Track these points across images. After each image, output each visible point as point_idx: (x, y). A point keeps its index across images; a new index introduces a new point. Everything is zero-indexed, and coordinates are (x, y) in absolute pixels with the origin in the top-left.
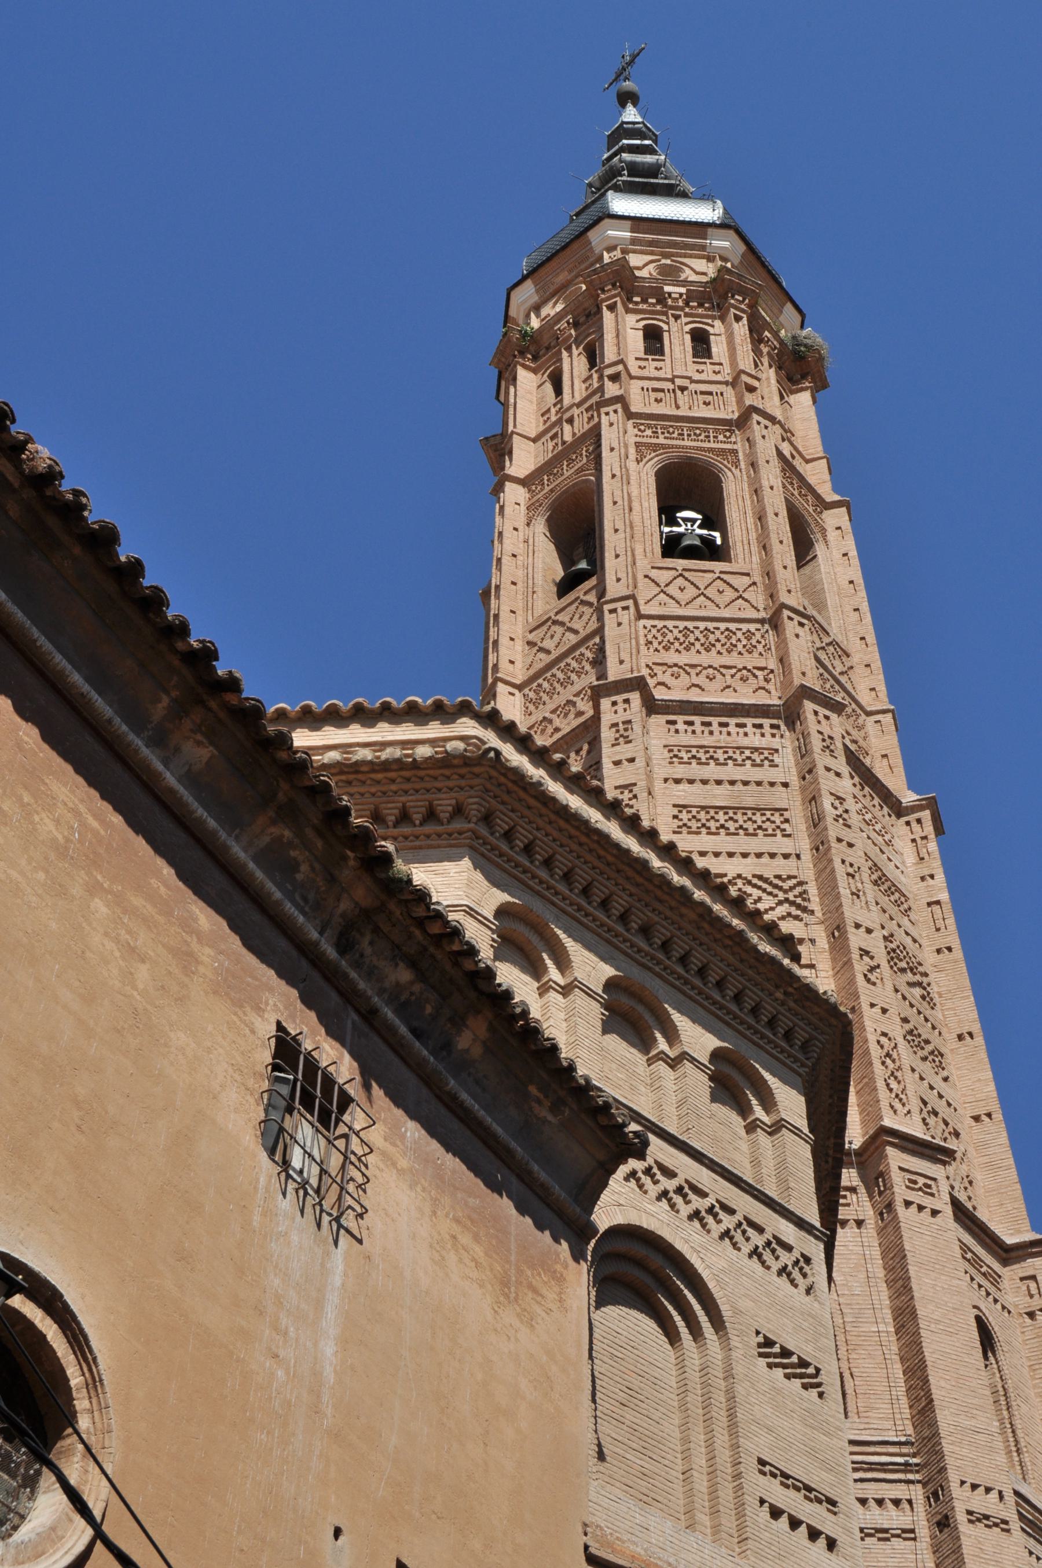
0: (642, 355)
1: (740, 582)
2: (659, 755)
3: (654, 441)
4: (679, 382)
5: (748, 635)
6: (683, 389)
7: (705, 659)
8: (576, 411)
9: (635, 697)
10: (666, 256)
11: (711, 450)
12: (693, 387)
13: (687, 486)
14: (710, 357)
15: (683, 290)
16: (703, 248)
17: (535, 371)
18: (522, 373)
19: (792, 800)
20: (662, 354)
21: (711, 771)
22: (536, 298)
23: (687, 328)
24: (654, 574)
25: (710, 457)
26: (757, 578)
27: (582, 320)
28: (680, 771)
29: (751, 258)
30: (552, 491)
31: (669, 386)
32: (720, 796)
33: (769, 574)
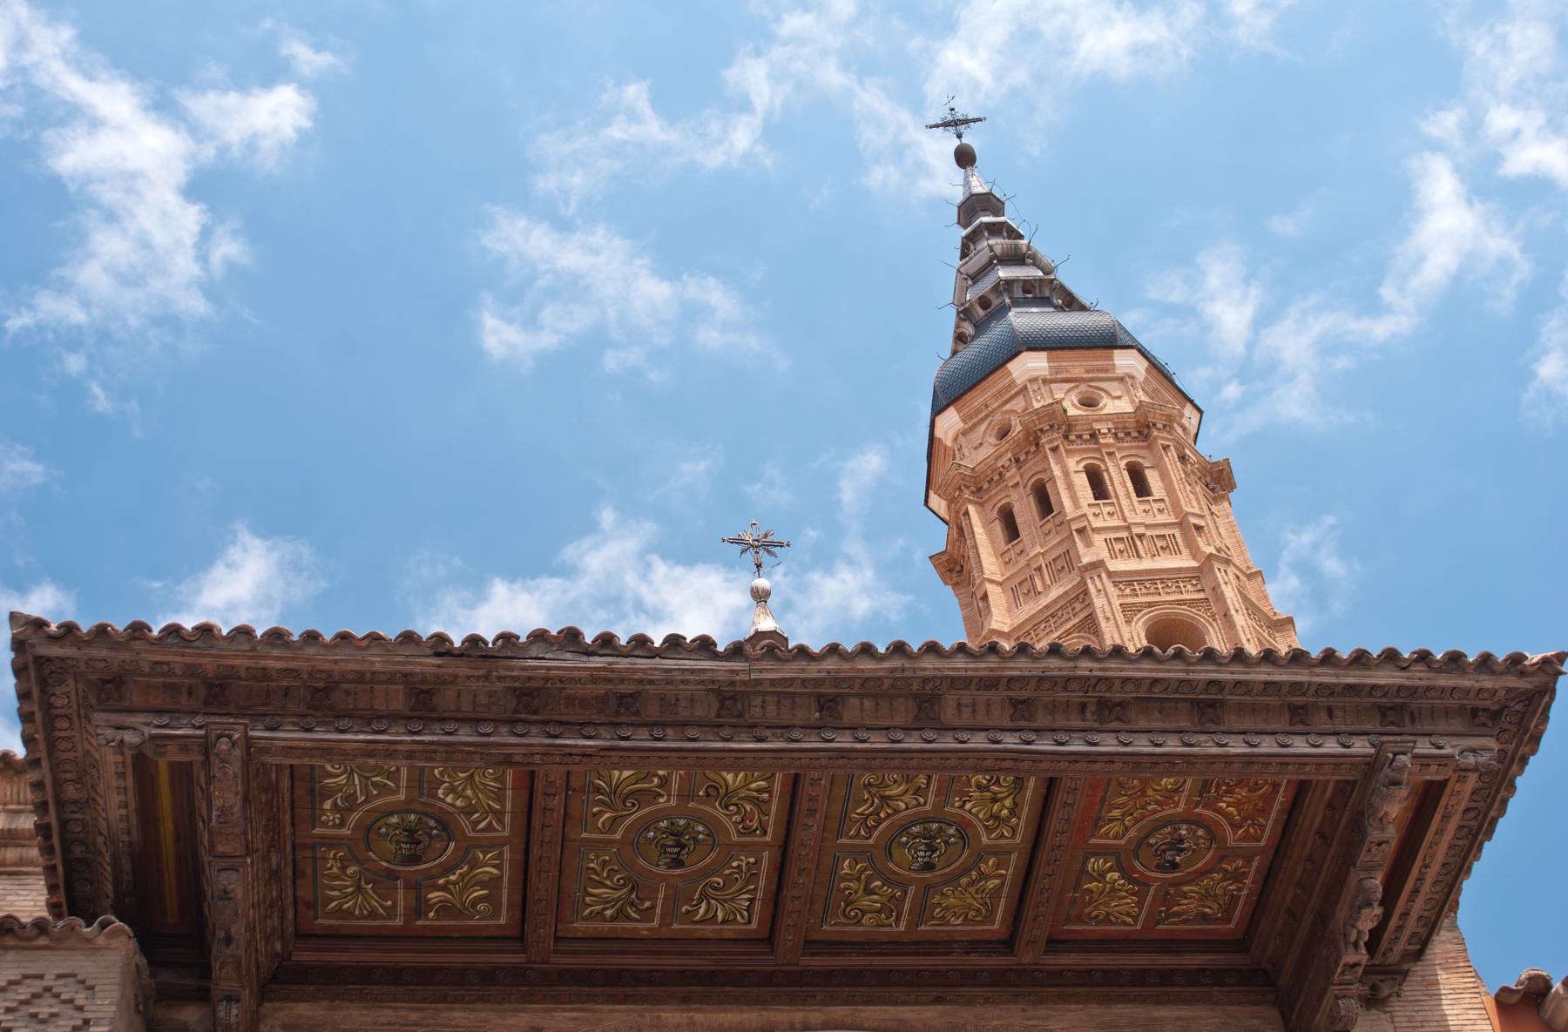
0: (1093, 501)
4: (1136, 530)
6: (1140, 536)
12: (1149, 533)
14: (1149, 494)
23: (1123, 464)
25: (1184, 610)
27: (1022, 458)
29: (1155, 372)
31: (1125, 534)
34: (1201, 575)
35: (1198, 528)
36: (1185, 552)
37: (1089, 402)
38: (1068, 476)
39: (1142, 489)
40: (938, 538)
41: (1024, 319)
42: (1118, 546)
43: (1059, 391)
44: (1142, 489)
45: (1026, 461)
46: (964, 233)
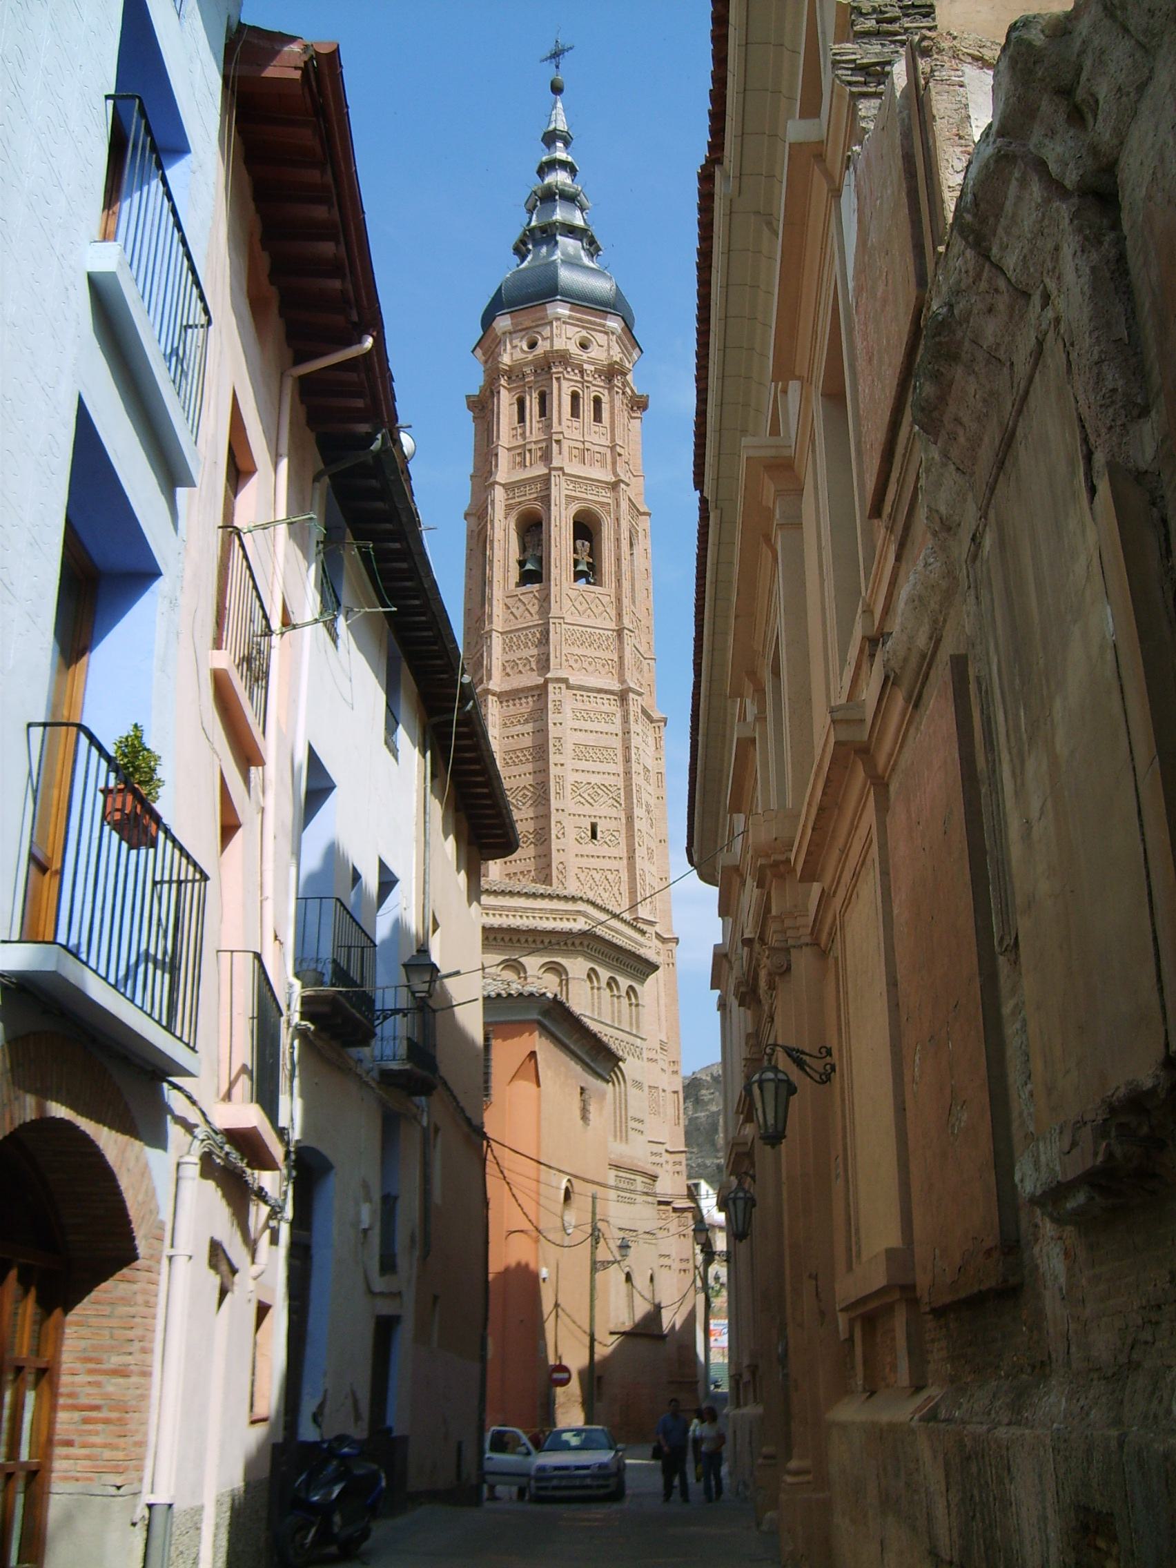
0: (569, 416)
1: (605, 600)
2: (569, 714)
3: (573, 494)
4: (587, 445)
5: (608, 638)
7: (590, 652)
8: (533, 446)
9: (563, 686)
10: (583, 327)
11: (599, 503)
13: (586, 529)
14: (600, 421)
15: (592, 368)
16: (604, 326)
17: (509, 390)
18: (503, 392)
19: (617, 743)
20: (578, 417)
21: (588, 725)
22: (510, 328)
23: (593, 395)
24: (570, 592)
26: (613, 599)
28: (577, 725)
30: (520, 503)
32: (591, 739)
33: (619, 600)
34: (614, 486)
35: (620, 455)
36: (609, 467)
37: (584, 346)
38: (562, 392)
39: (598, 417)
40: (475, 384)
41: (560, 214)
42: (575, 452)
43: (571, 331)
44: (598, 417)
45: (539, 375)
46: (544, 159)
